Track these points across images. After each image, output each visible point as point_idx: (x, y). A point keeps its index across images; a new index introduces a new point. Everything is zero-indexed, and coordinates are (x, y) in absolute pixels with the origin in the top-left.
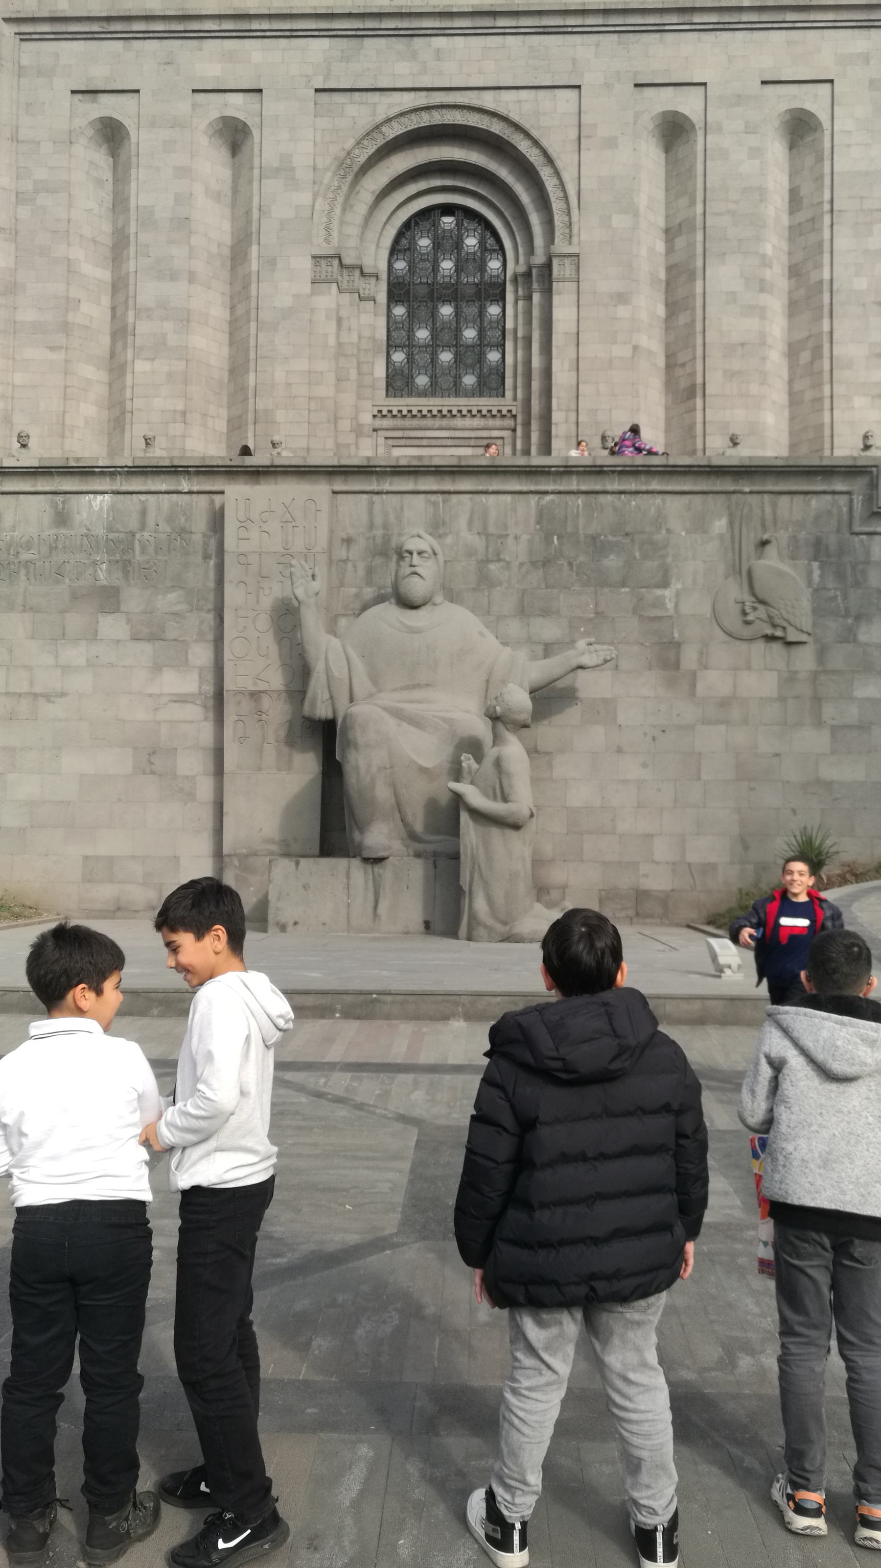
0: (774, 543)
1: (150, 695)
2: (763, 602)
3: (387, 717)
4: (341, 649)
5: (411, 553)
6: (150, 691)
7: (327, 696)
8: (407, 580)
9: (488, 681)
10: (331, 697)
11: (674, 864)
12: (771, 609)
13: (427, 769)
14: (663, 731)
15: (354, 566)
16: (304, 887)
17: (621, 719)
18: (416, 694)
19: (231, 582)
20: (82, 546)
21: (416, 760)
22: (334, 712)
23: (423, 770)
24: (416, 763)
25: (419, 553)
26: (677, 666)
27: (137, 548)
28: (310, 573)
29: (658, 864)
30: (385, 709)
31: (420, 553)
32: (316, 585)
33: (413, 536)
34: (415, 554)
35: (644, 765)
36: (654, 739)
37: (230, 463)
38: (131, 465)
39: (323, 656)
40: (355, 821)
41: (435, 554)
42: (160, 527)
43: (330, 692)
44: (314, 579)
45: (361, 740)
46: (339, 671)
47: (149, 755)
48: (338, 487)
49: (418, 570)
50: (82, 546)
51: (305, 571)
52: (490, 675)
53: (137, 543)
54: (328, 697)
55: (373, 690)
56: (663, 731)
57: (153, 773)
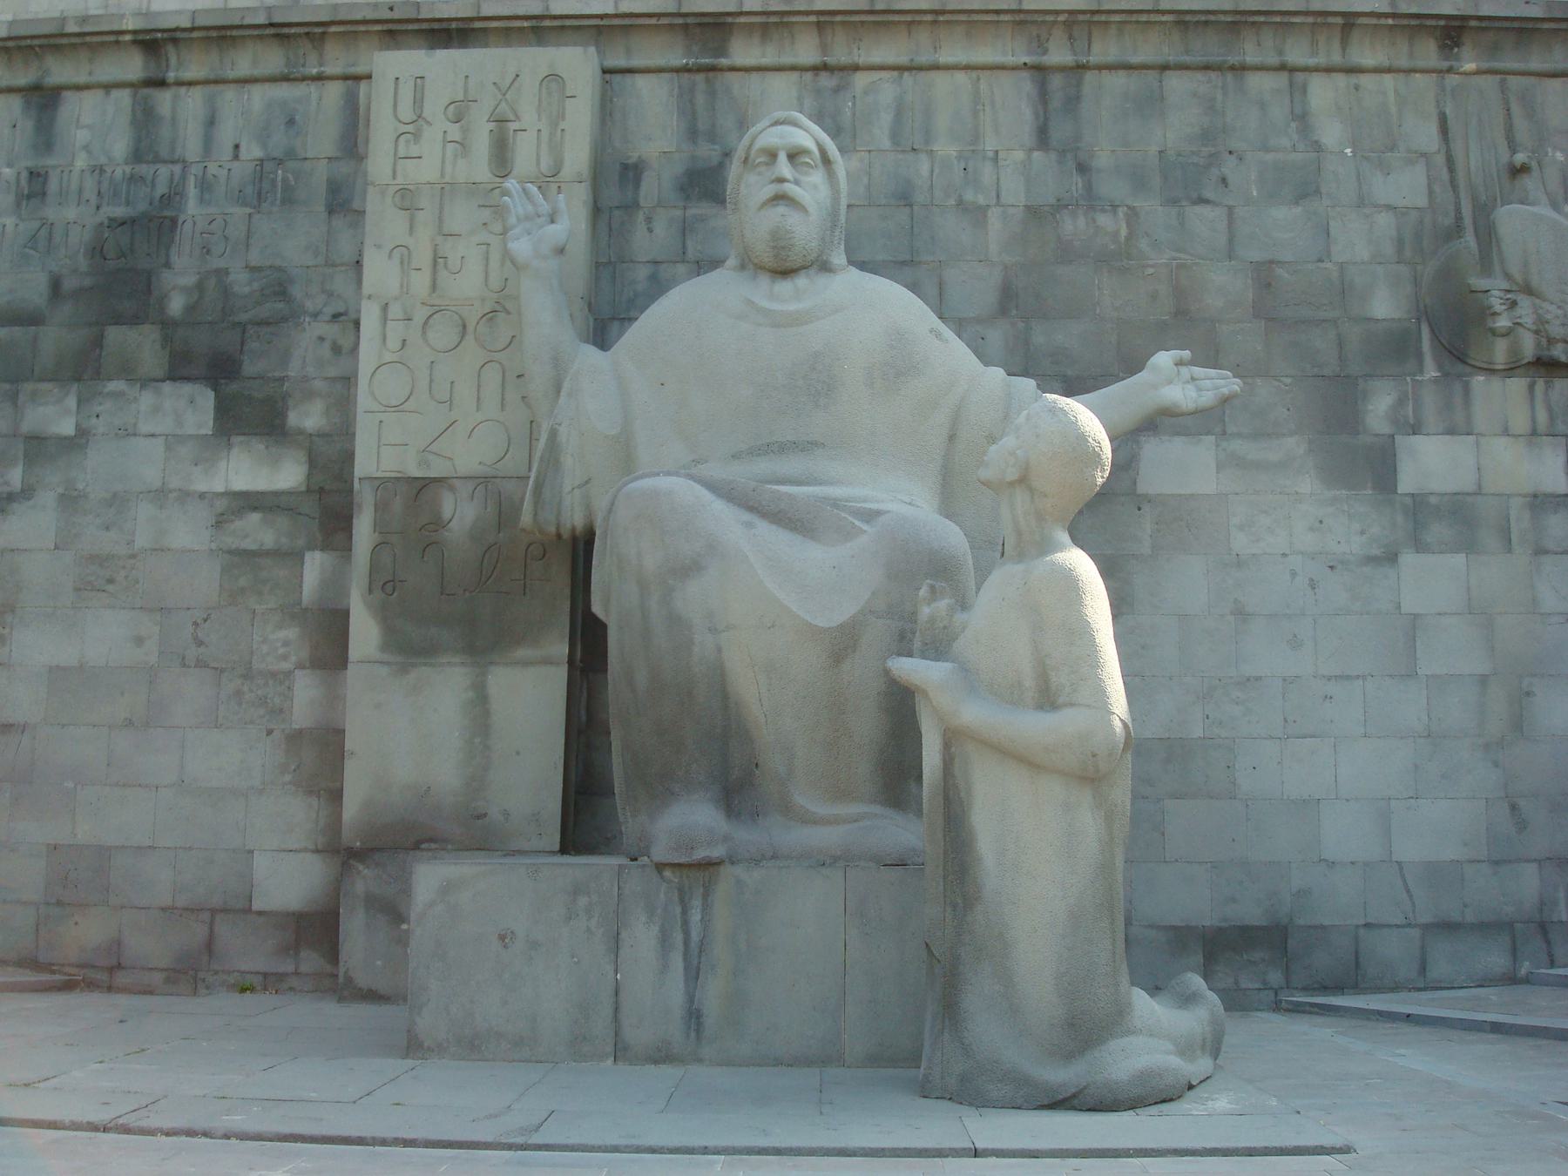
0: (1535, 173)
1: (202, 496)
2: (1528, 290)
3: (718, 506)
5: (772, 155)
6: (201, 487)
11: (1366, 864)
12: (1546, 305)
14: (1331, 567)
15: (649, 220)
16: (502, 938)
17: (1240, 542)
18: (791, 465)
19: (378, 247)
20: (80, 191)
25: (792, 157)
27: (192, 191)
28: (545, 207)
29: (1332, 864)
30: (713, 487)
31: (794, 156)
32: (558, 231)
33: (777, 123)
34: (782, 157)
35: (1295, 643)
36: (1313, 585)
37: (388, 15)
38: (188, 25)
41: (826, 161)
42: (243, 149)
47: (196, 624)
48: (611, 63)
49: (790, 188)
50: (80, 191)
53: (191, 181)
56: (1331, 567)
57: (201, 664)
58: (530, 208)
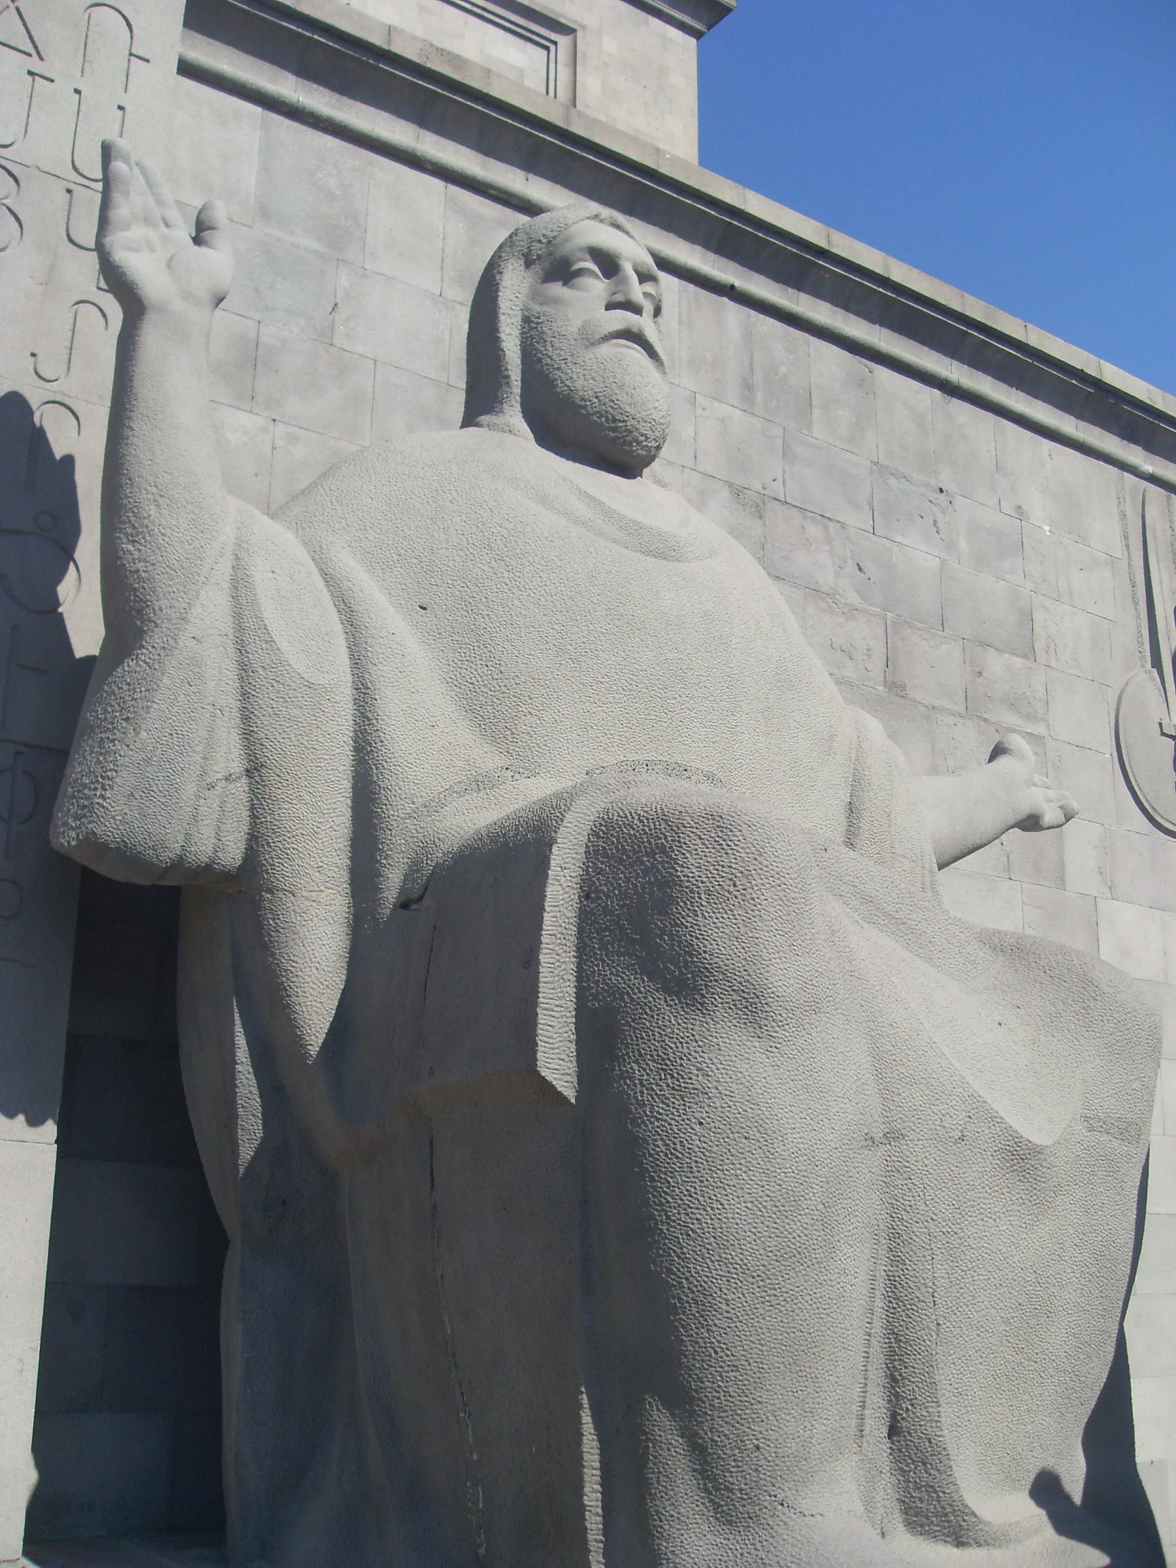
4: (304, 556)
7: (229, 756)
8: (607, 350)
9: (851, 809)
10: (254, 770)
13: (1038, 1151)
21: (987, 1097)
22: (255, 840)
23: (1020, 1158)
24: (994, 1119)
26: (1060, 879)
33: (596, 217)
39: (223, 571)
40: (702, 1455)
43: (249, 737)
44: (198, 240)
45: (782, 977)
46: (308, 649)
49: (644, 323)
51: (159, 201)
52: (857, 783)
54: (237, 765)
55: (490, 760)
58: (150, 200)
